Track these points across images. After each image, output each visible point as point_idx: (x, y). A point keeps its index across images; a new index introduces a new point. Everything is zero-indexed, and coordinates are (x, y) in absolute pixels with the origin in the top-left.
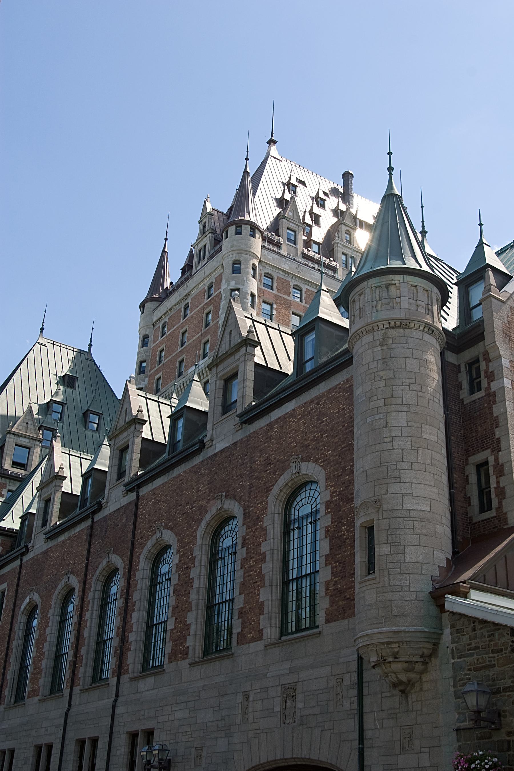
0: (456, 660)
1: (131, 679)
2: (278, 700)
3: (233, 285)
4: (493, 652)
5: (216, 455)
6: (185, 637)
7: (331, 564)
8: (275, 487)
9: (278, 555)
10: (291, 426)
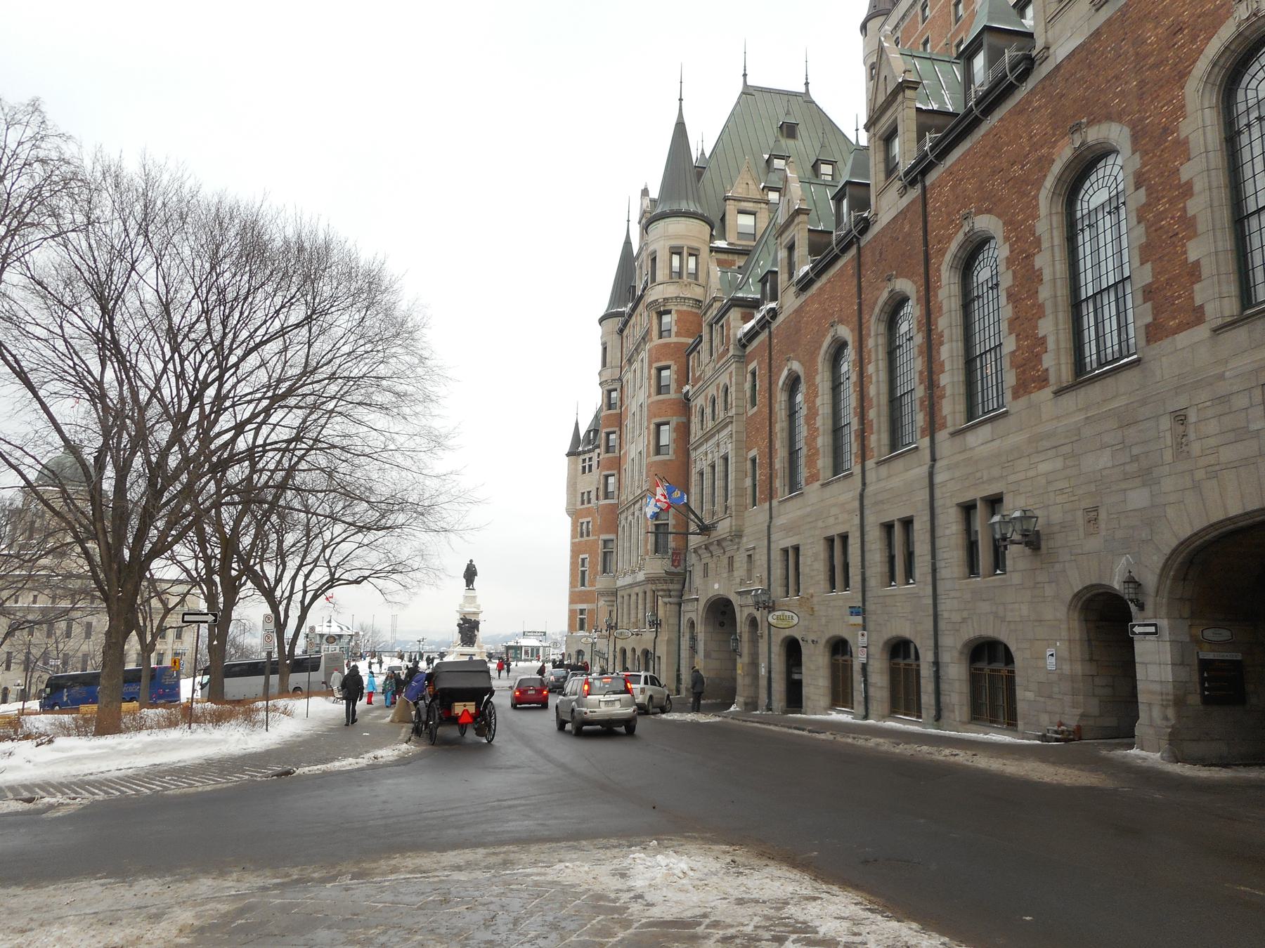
1: (956, 434)
5: (1058, 67)
6: (1038, 358)
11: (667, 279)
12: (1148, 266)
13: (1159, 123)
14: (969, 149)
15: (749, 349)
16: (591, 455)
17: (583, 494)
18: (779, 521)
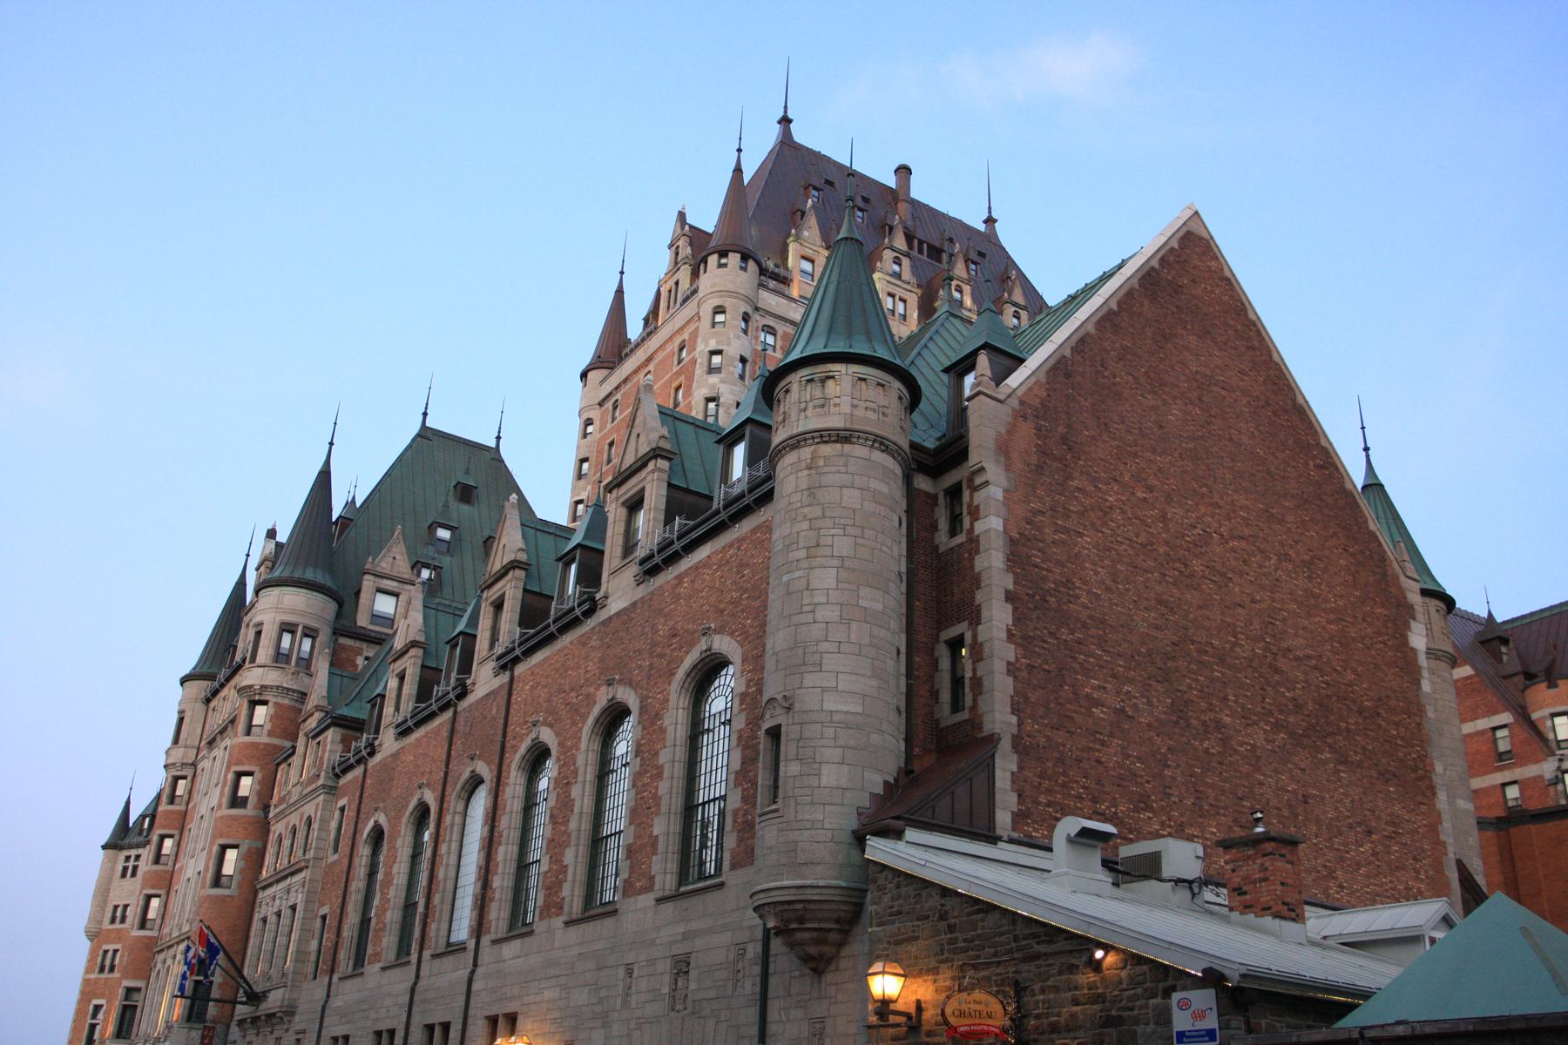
0: (875, 929)
1: (494, 942)
2: (667, 978)
3: (713, 345)
4: (918, 919)
5: (610, 619)
9: (679, 770)
10: (704, 580)
11: (268, 662)
12: (633, 827)
15: (342, 781)
16: (140, 851)
17: (116, 907)
18: (336, 1003)
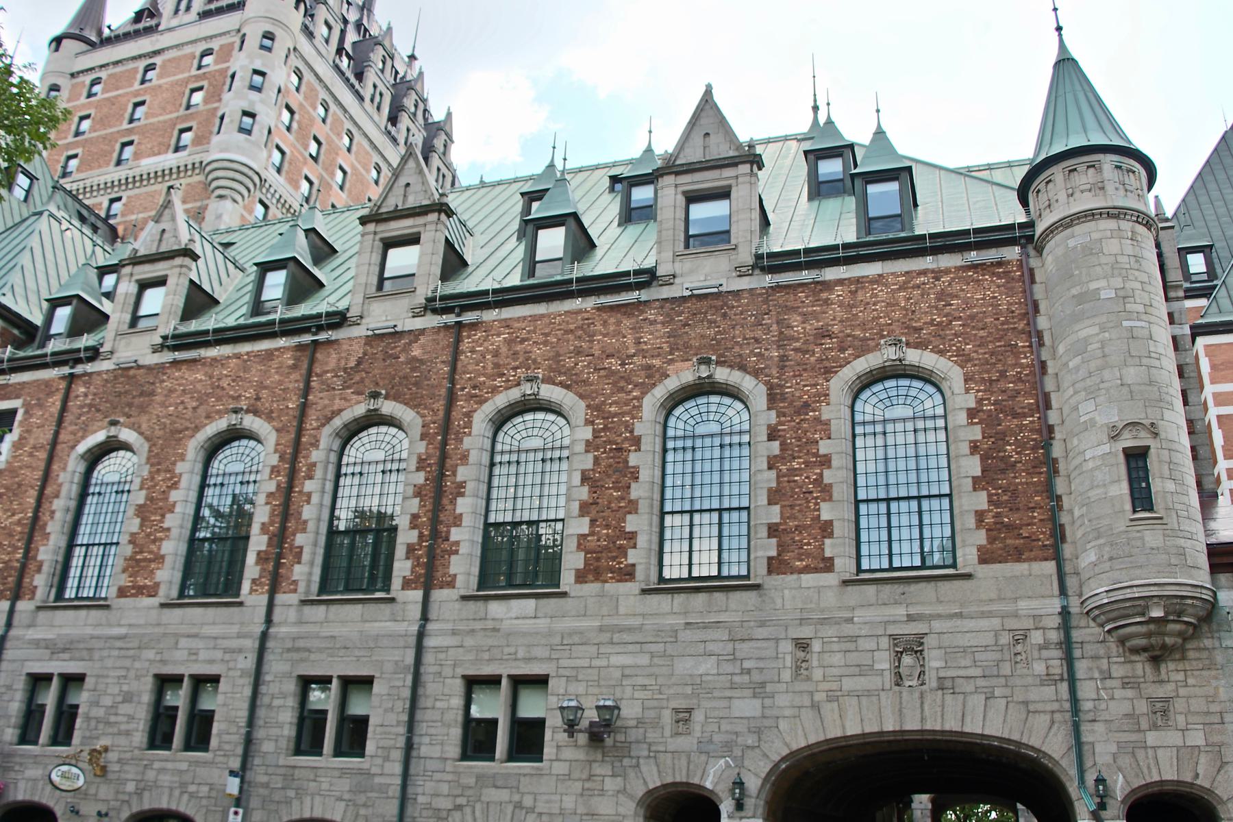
2: (885, 655)
6: (623, 551)
7: (987, 489)
8: (844, 369)
10: (876, 296)
13: (801, 397)
14: (542, 316)
